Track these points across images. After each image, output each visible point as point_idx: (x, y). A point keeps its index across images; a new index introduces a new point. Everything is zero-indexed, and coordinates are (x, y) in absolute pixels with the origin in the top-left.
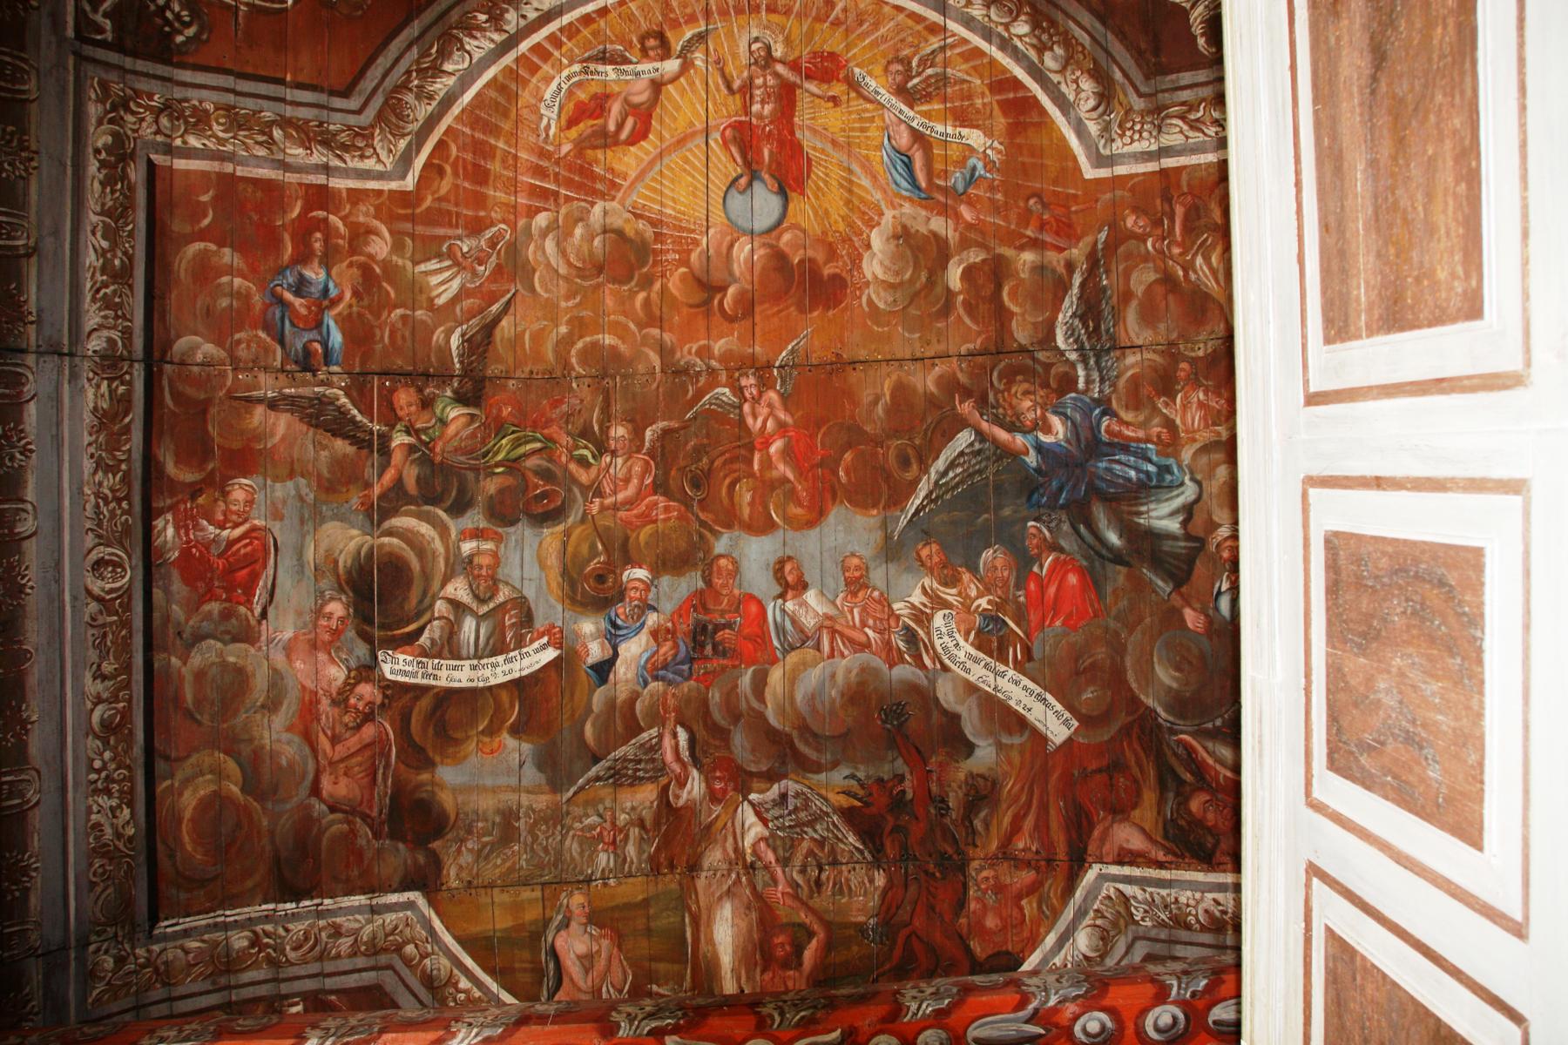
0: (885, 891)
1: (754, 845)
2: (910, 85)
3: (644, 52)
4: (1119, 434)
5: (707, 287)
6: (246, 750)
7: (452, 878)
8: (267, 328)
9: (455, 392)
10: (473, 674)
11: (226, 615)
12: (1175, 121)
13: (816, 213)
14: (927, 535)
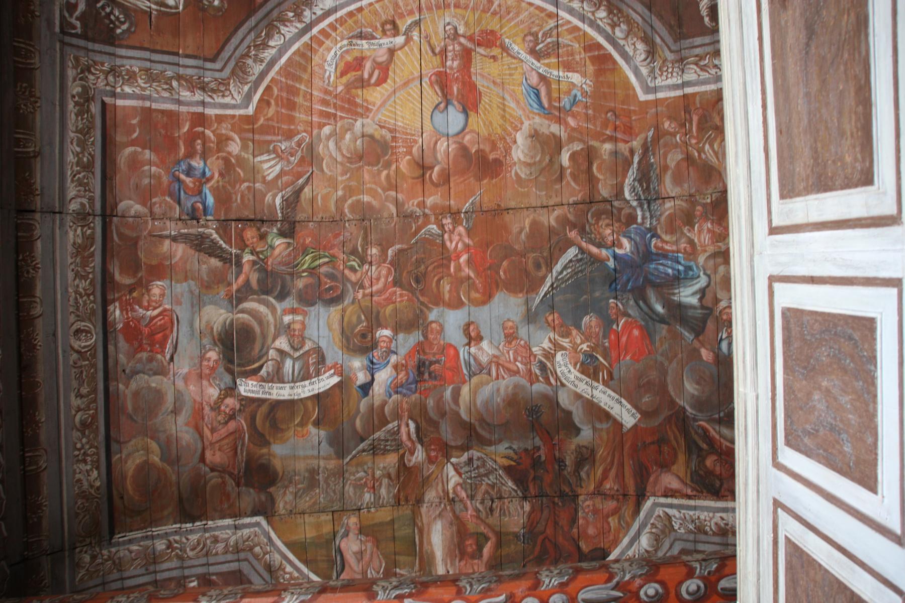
0: (530, 514)
1: (454, 489)
2: (537, 48)
3: (384, 32)
4: (662, 248)
5: (423, 167)
6: (163, 437)
7: (281, 507)
8: (171, 195)
9: (279, 230)
10: (291, 392)
11: (151, 360)
12: (692, 66)
13: (485, 124)
14: (552, 308)
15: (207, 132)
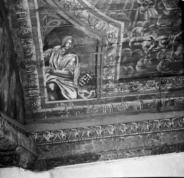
15: (132, 40)
